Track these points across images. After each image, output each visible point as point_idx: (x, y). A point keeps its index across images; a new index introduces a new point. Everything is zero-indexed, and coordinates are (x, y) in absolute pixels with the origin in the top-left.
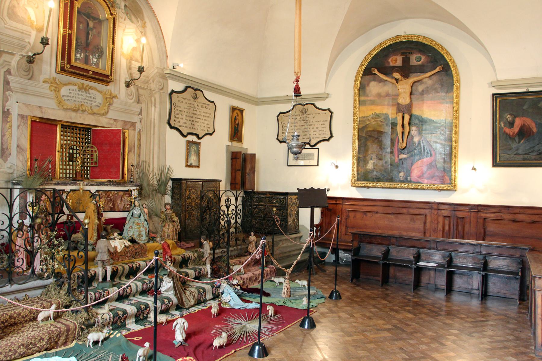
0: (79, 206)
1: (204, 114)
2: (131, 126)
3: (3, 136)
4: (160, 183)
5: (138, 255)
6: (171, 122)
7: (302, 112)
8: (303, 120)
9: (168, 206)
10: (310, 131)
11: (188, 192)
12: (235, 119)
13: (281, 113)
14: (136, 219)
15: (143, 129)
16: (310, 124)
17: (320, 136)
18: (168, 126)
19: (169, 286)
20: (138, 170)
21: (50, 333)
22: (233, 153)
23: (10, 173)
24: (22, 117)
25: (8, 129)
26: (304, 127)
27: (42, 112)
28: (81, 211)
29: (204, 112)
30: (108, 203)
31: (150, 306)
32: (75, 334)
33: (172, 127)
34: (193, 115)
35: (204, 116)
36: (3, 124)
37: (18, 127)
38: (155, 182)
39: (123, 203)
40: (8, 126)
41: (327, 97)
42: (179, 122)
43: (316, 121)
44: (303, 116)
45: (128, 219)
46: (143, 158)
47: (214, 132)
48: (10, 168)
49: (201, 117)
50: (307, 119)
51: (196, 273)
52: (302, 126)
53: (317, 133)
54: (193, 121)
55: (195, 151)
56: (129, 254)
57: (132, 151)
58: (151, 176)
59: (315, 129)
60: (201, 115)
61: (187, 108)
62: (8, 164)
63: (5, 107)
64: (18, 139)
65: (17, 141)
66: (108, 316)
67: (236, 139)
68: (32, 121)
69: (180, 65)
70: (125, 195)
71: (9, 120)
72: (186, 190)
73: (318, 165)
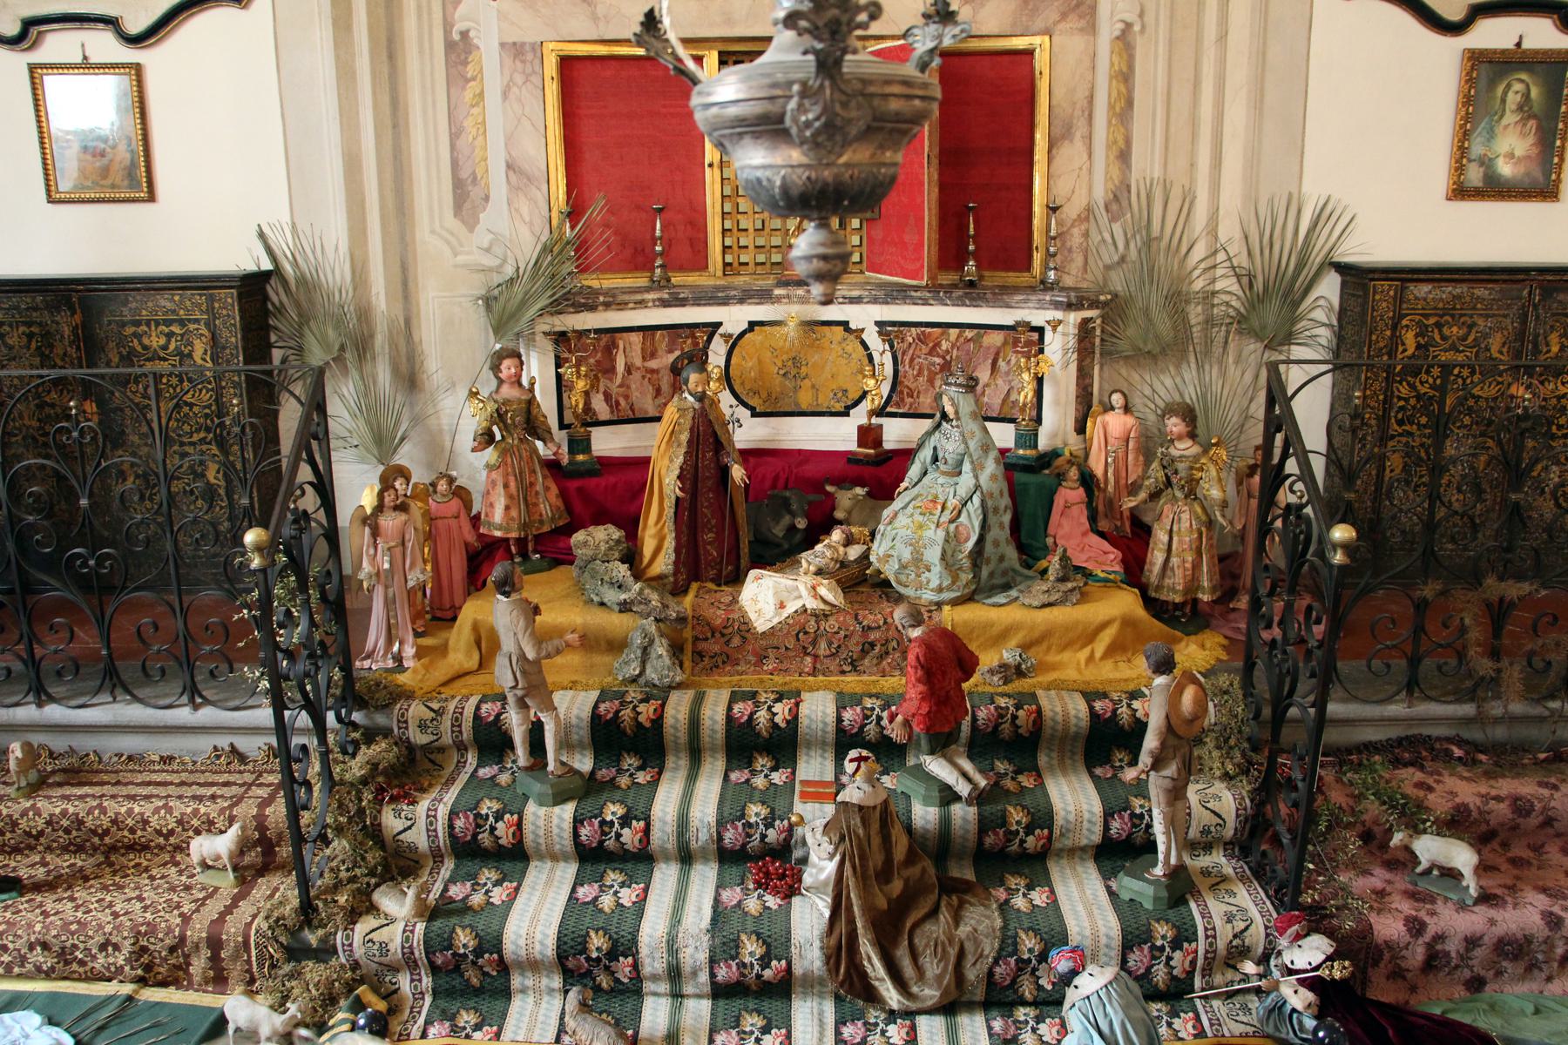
0: (796, 389)
2: (1064, 16)
3: (455, 136)
4: (1259, 285)
5: (881, 657)
9: (1174, 420)
11: (1410, 339)
14: (941, 480)
15: (1150, 18)
19: (823, 876)
20: (1117, 228)
21: (139, 933)
23: (491, 270)
24: (515, 50)
25: (473, 106)
27: (595, 18)
28: (804, 407)
30: (931, 381)
31: (644, 951)
32: (249, 962)
36: (453, 91)
37: (505, 94)
38: (1228, 284)
39: (1000, 382)
40: (468, 95)
45: (914, 471)
46: (1146, 164)
48: (488, 250)
51: (1116, 825)
55: (1524, 106)
56: (823, 645)
57: (1078, 135)
58: (1199, 251)
62: (482, 237)
63: (452, 26)
64: (509, 140)
65: (506, 144)
66: (398, 940)
68: (567, 64)
70: (1009, 349)
71: (470, 71)
72: (1395, 327)
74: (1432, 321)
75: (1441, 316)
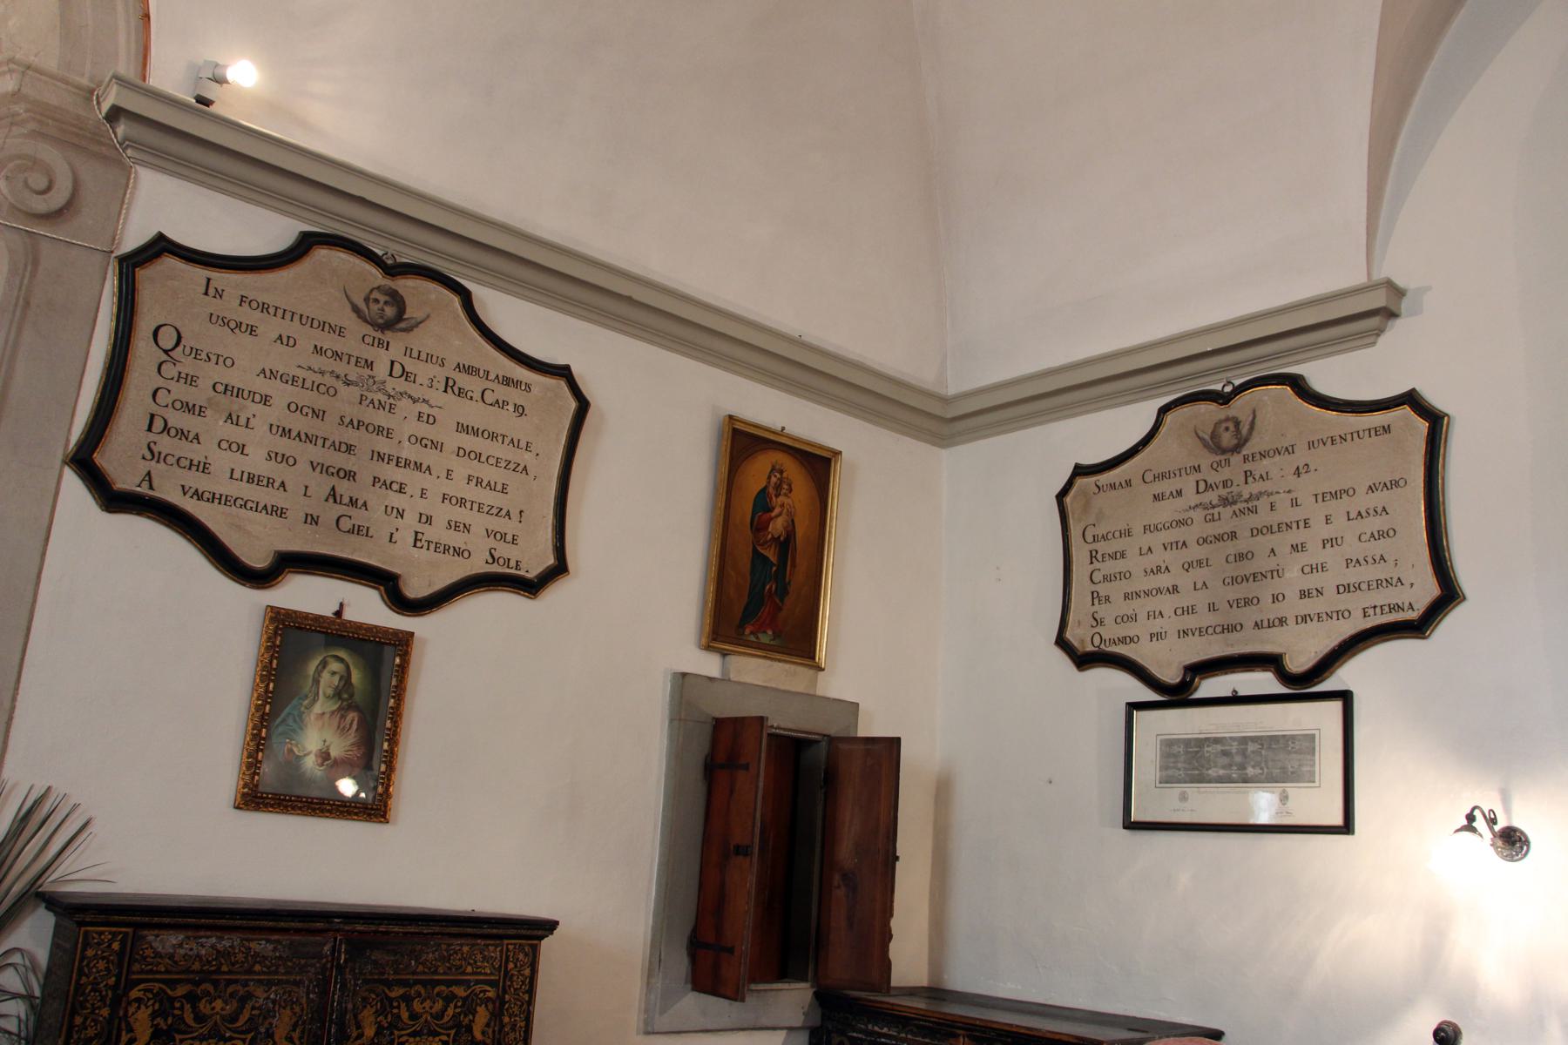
1: (469, 442)
6: (109, 459)
7: (1213, 444)
8: (1225, 502)
10: (1276, 573)
12: (763, 503)
13: (1080, 471)
16: (1274, 519)
17: (1356, 602)
18: (73, 487)
22: (719, 724)
26: (1231, 548)
29: (463, 428)
33: (114, 500)
34: (350, 436)
35: (461, 452)
41: (1390, 314)
42: (204, 467)
43: (1323, 497)
44: (1225, 473)
47: (560, 568)
49: (429, 457)
50: (1254, 487)
52: (1219, 538)
53: (1328, 581)
54: (350, 475)
59: (1315, 555)
60: (437, 446)
61: (283, 378)
67: (765, 639)
69: (231, 74)
73: (1347, 827)
74: (181, 991)
75: (197, 984)
